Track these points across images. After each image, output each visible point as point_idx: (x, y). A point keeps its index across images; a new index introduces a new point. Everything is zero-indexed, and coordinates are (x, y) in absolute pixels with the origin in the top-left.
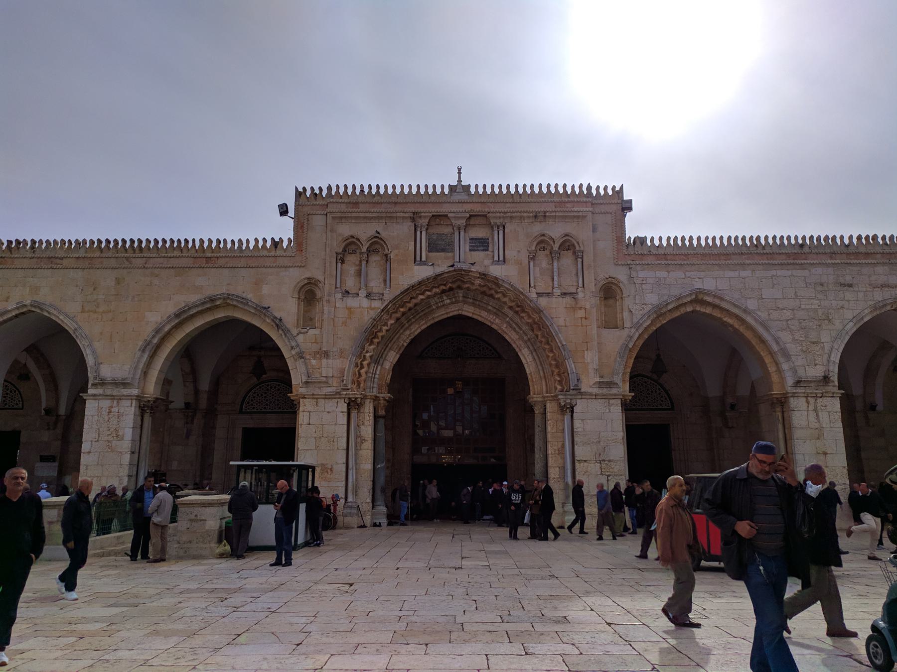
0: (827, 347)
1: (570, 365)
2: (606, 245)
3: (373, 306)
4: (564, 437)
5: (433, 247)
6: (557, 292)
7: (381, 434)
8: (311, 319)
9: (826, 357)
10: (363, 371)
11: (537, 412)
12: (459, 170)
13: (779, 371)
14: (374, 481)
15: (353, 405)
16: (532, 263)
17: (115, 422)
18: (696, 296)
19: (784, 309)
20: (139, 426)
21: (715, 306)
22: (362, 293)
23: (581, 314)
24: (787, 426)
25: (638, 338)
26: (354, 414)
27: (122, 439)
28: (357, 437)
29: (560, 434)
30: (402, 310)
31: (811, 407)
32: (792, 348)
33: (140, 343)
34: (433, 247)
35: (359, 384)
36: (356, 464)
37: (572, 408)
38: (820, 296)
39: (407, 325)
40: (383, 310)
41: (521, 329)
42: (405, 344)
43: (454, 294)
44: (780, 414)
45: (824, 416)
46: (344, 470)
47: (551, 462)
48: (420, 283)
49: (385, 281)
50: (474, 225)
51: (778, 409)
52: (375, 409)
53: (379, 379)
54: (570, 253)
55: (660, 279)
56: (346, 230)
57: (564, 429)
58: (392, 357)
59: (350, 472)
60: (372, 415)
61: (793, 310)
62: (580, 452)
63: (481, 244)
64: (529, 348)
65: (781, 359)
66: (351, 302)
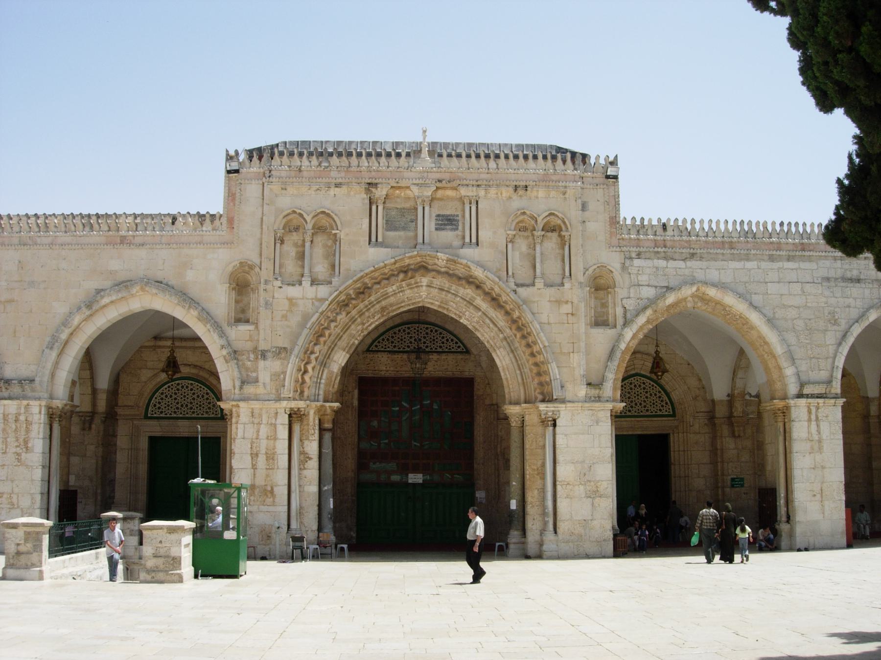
0: (831, 349)
1: (554, 370)
2: (597, 226)
3: (320, 296)
4: (544, 455)
5: (390, 225)
6: (539, 283)
7: (328, 450)
8: (243, 311)
9: (830, 360)
10: (307, 378)
11: (513, 425)
12: (425, 132)
13: (782, 377)
14: (320, 506)
15: (295, 417)
16: (510, 245)
17: (23, 433)
18: (698, 289)
19: (790, 307)
20: (48, 437)
21: (718, 303)
22: (306, 282)
23: (566, 308)
24: (787, 438)
25: (633, 338)
26: (296, 428)
27: (33, 451)
28: (302, 453)
29: (539, 451)
30: (354, 302)
31: (813, 417)
32: (799, 353)
33: (48, 339)
34: (390, 225)
35: (302, 392)
36: (300, 486)
37: (555, 420)
38: (827, 293)
39: (359, 320)
40: (331, 303)
41: (496, 326)
42: (357, 342)
43: (416, 283)
44: (781, 425)
45: (824, 426)
46: (286, 492)
47: (528, 483)
48: (376, 270)
49: (333, 266)
50: (441, 199)
51: (780, 419)
52: (320, 420)
53: (326, 385)
54: (554, 235)
55: (657, 268)
56: (286, 202)
57: (544, 446)
58: (340, 359)
59: (293, 496)
60: (317, 427)
61: (798, 308)
62: (563, 472)
63: (447, 222)
64: (505, 348)
65: (784, 363)
66: (293, 292)
